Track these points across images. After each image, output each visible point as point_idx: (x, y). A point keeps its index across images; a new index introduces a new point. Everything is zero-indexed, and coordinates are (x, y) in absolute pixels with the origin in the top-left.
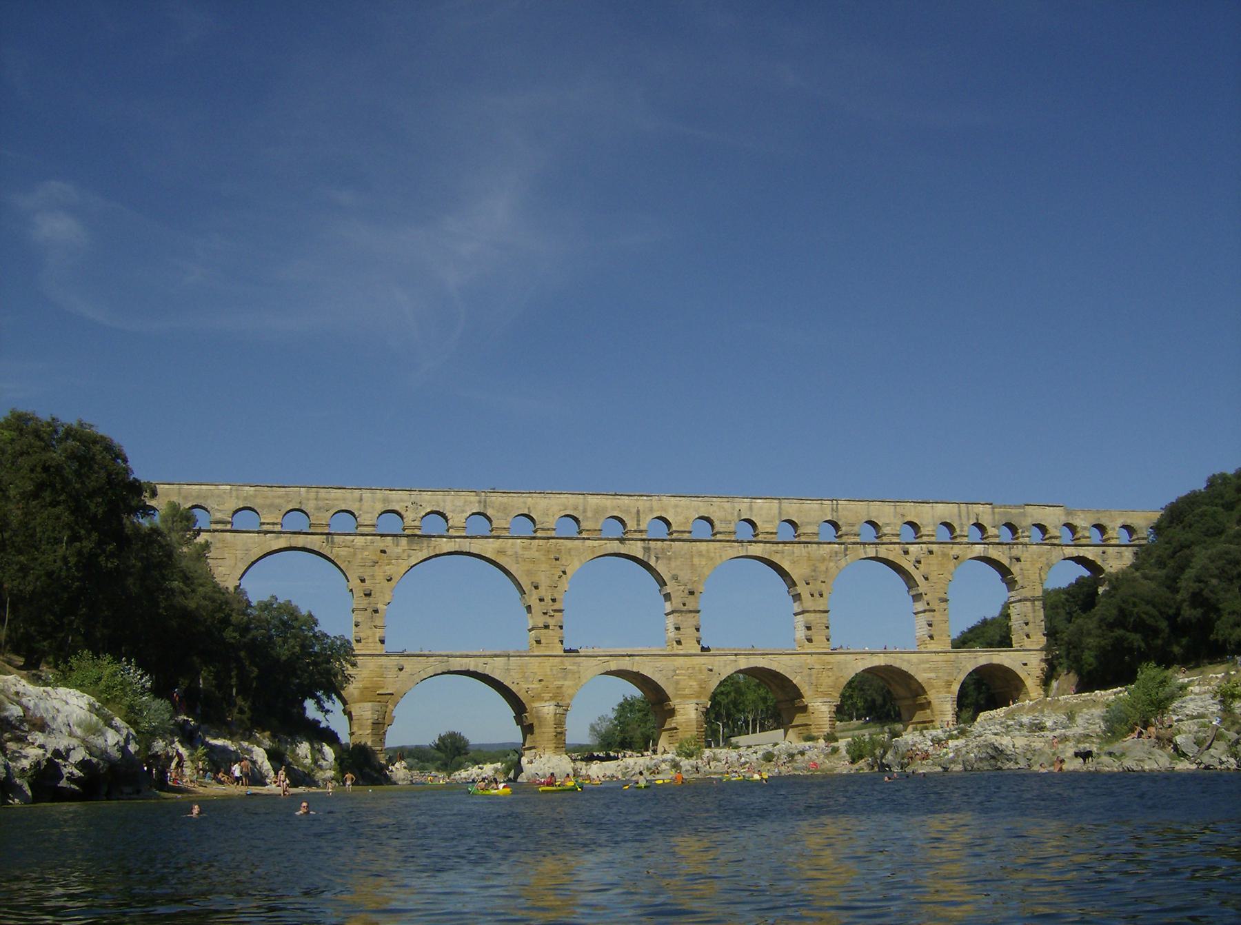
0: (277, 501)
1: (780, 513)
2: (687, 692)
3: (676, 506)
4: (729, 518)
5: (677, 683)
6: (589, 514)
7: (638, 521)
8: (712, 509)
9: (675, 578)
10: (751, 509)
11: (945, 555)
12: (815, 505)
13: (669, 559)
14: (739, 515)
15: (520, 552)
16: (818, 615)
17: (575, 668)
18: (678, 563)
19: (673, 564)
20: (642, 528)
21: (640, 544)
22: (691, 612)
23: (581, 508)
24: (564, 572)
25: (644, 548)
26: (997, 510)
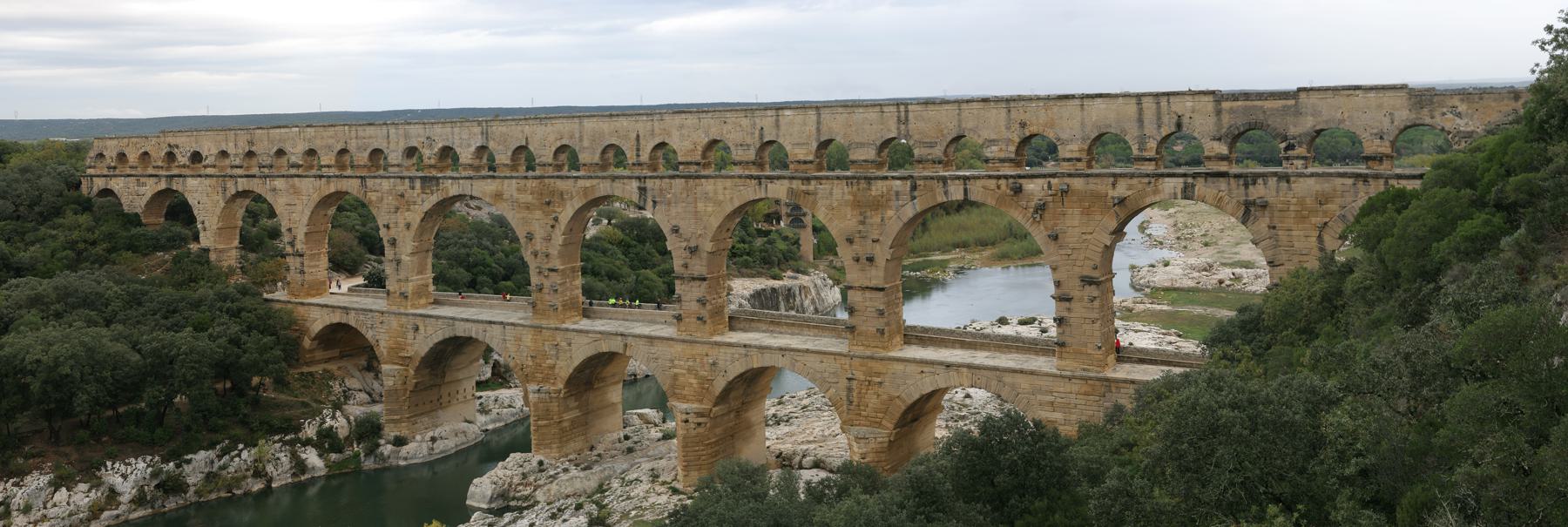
0: (331, 141)
1: (818, 130)
3: (682, 127)
4: (749, 141)
5: (675, 377)
6: (586, 143)
8: (726, 128)
9: (676, 230)
10: (777, 125)
11: (1099, 197)
12: (873, 115)
14: (761, 136)
15: (515, 195)
16: (868, 294)
19: (673, 211)
21: (635, 184)
22: (694, 279)
24: (556, 219)
25: (640, 188)
26: (1226, 105)
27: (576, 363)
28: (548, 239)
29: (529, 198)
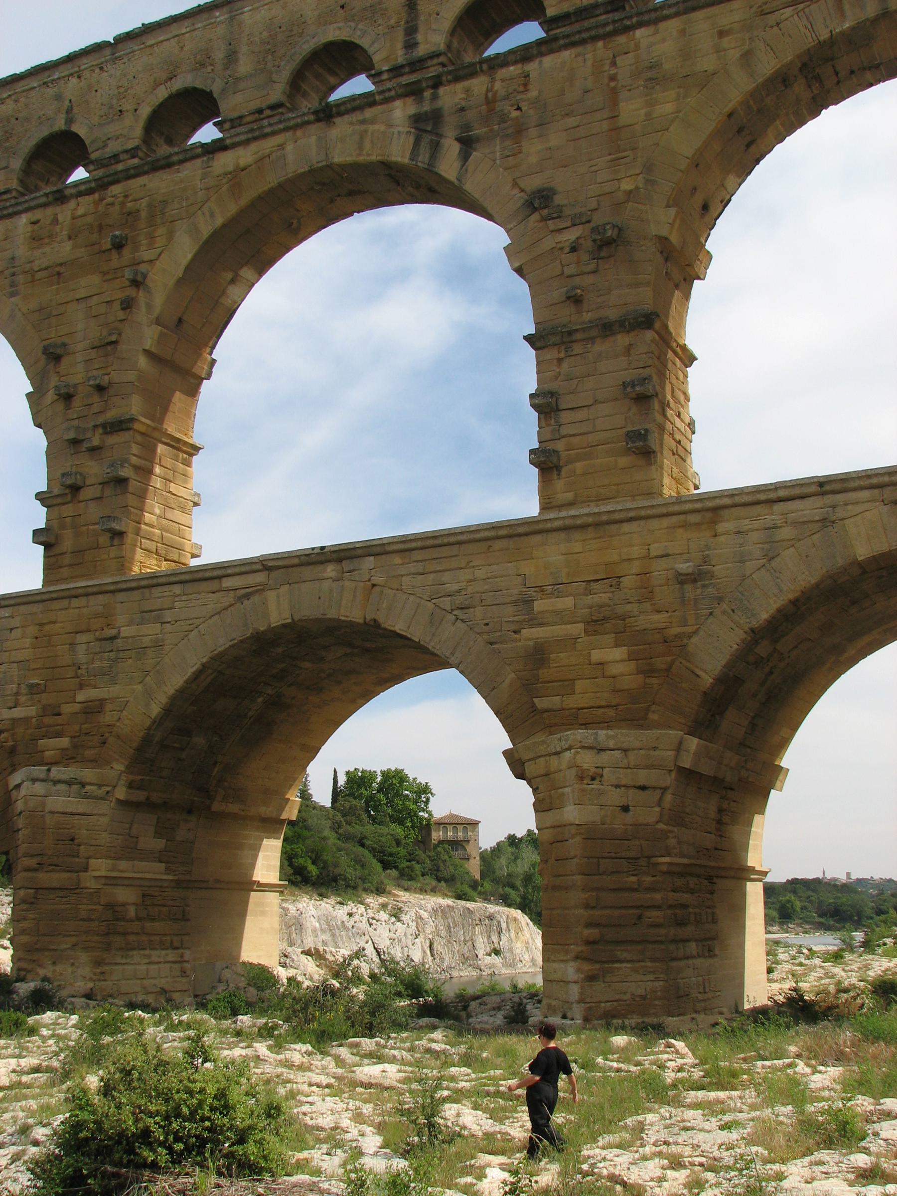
2: (583, 695)
6: (244, 66)
7: (411, 31)
13: (519, 131)
17: (151, 630)
18: (555, 139)
19: (533, 149)
20: (422, 50)
21: (401, 111)
22: (607, 328)
23: (219, 55)
25: (417, 120)
27: (176, 681)
28: (108, 346)
29: (64, 250)
